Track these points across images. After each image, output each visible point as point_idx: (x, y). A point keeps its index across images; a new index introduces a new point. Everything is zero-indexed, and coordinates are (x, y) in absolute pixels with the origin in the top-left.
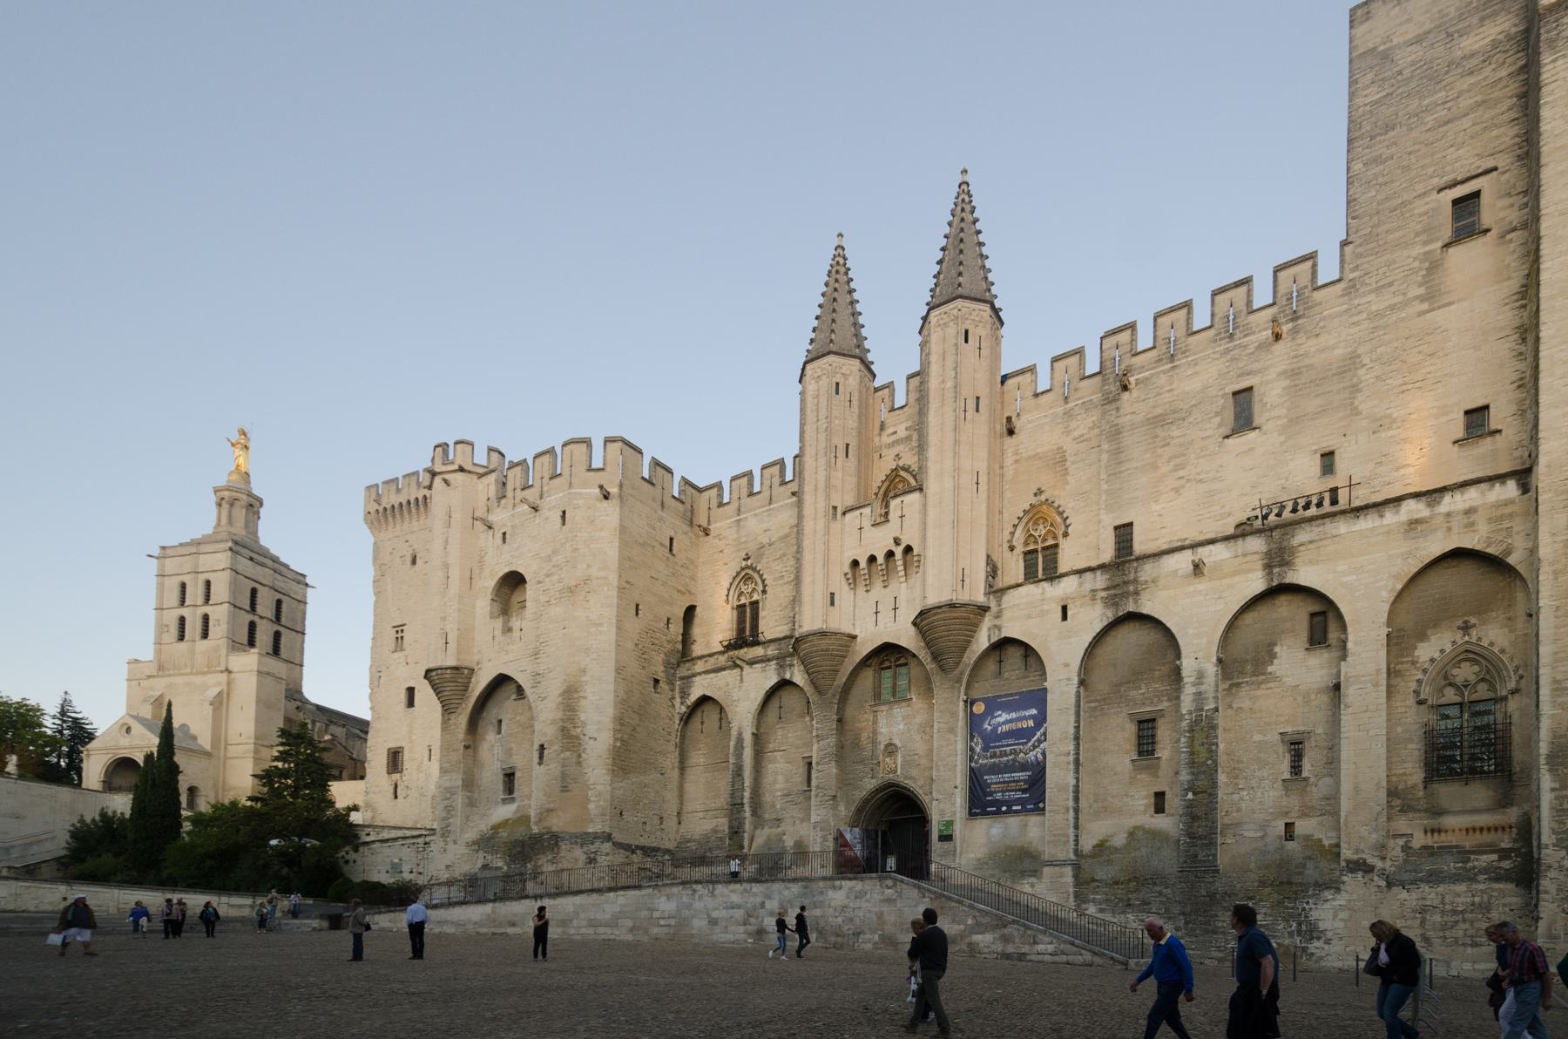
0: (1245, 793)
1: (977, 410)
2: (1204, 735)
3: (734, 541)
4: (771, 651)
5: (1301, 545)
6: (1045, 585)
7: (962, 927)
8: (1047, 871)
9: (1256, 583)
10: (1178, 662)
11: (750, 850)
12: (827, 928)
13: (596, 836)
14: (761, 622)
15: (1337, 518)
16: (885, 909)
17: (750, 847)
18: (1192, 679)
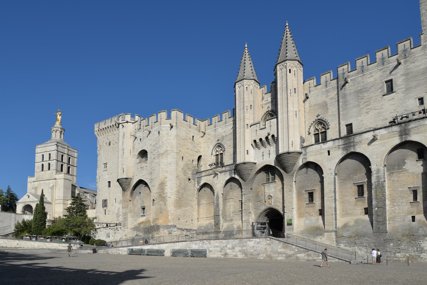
0: (397, 207)
1: (295, 92)
2: (381, 189)
3: (214, 135)
4: (227, 168)
5: (412, 128)
6: (321, 144)
7: (294, 252)
8: (326, 234)
9: (397, 141)
10: (370, 167)
11: (222, 229)
12: (248, 253)
13: (171, 226)
14: (224, 160)
15: (424, 119)
16: (267, 247)
17: (222, 228)
18: (375, 172)
